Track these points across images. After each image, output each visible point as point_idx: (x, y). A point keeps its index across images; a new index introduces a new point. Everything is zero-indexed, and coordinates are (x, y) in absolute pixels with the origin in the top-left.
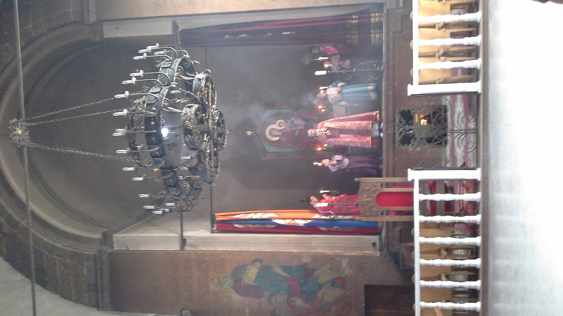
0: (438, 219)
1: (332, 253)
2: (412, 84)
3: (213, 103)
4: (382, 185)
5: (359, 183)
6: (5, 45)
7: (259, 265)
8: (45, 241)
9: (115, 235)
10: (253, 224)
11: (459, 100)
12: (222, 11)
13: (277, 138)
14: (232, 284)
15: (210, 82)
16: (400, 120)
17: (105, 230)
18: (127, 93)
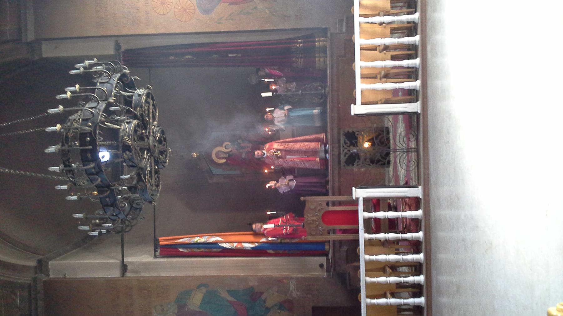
0: (381, 236)
1: (279, 276)
2: (355, 104)
3: (154, 119)
4: (328, 204)
5: (304, 202)
7: (204, 290)
9: (50, 263)
10: (199, 248)
11: (401, 122)
12: (166, 32)
13: (224, 161)
14: (176, 312)
15: (150, 98)
16: (345, 141)
17: (40, 257)
18: (61, 107)
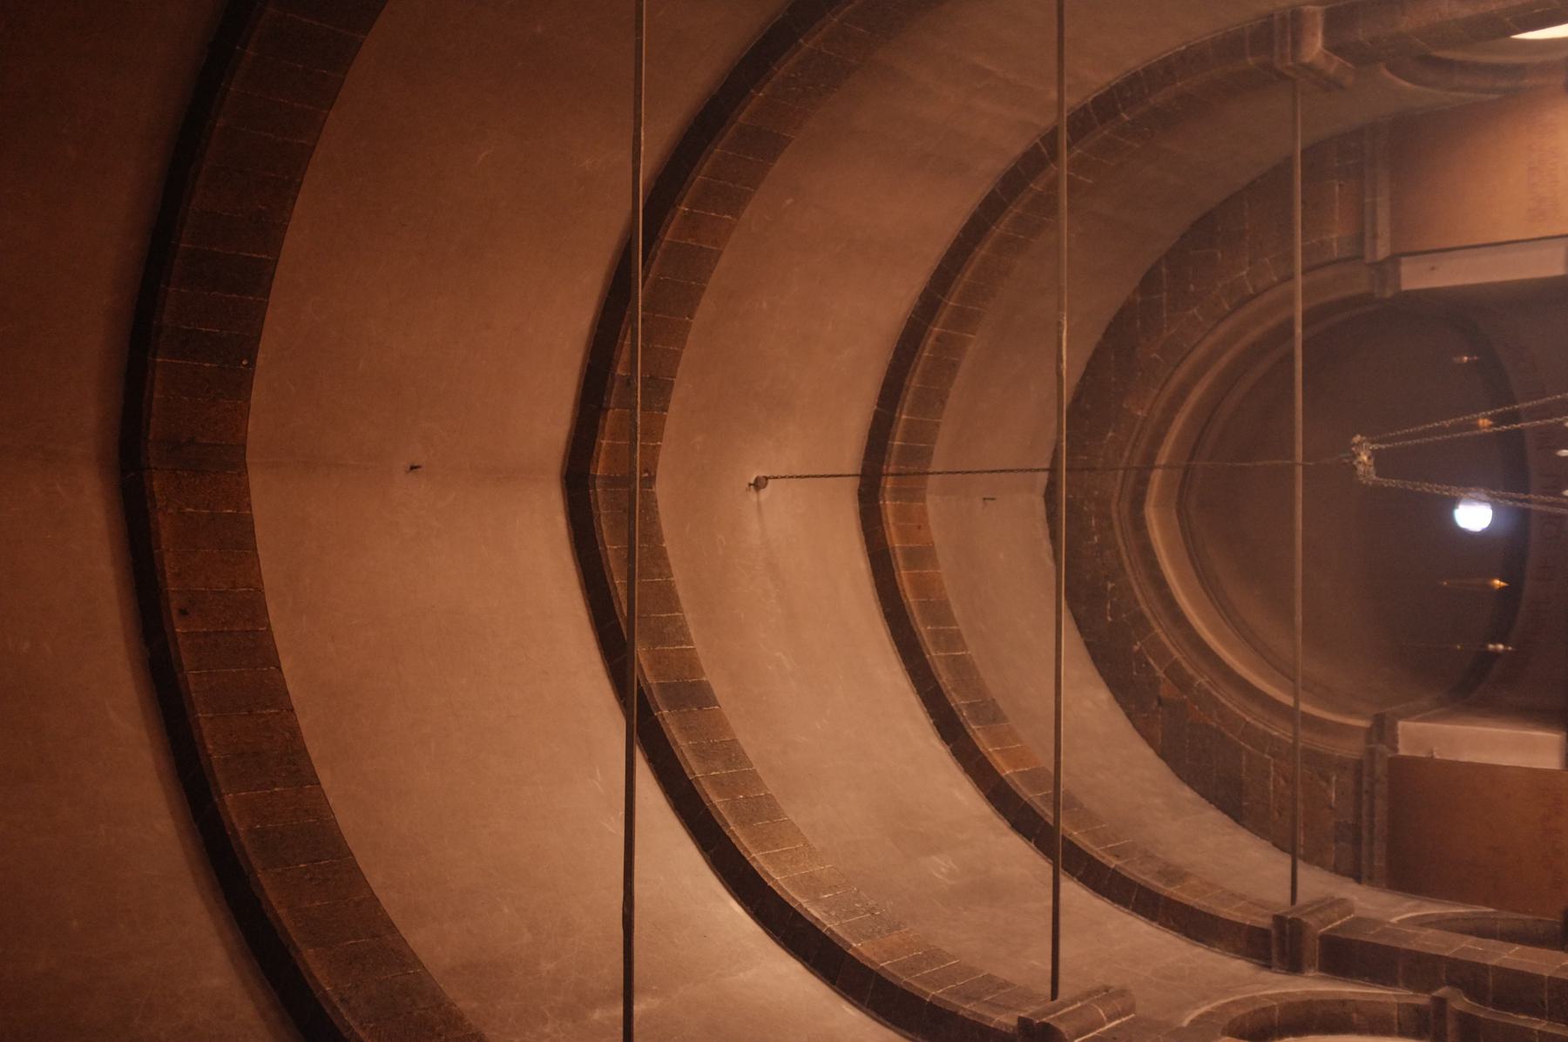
6: (1190, 312)
8: (1247, 723)
9: (1401, 724)
